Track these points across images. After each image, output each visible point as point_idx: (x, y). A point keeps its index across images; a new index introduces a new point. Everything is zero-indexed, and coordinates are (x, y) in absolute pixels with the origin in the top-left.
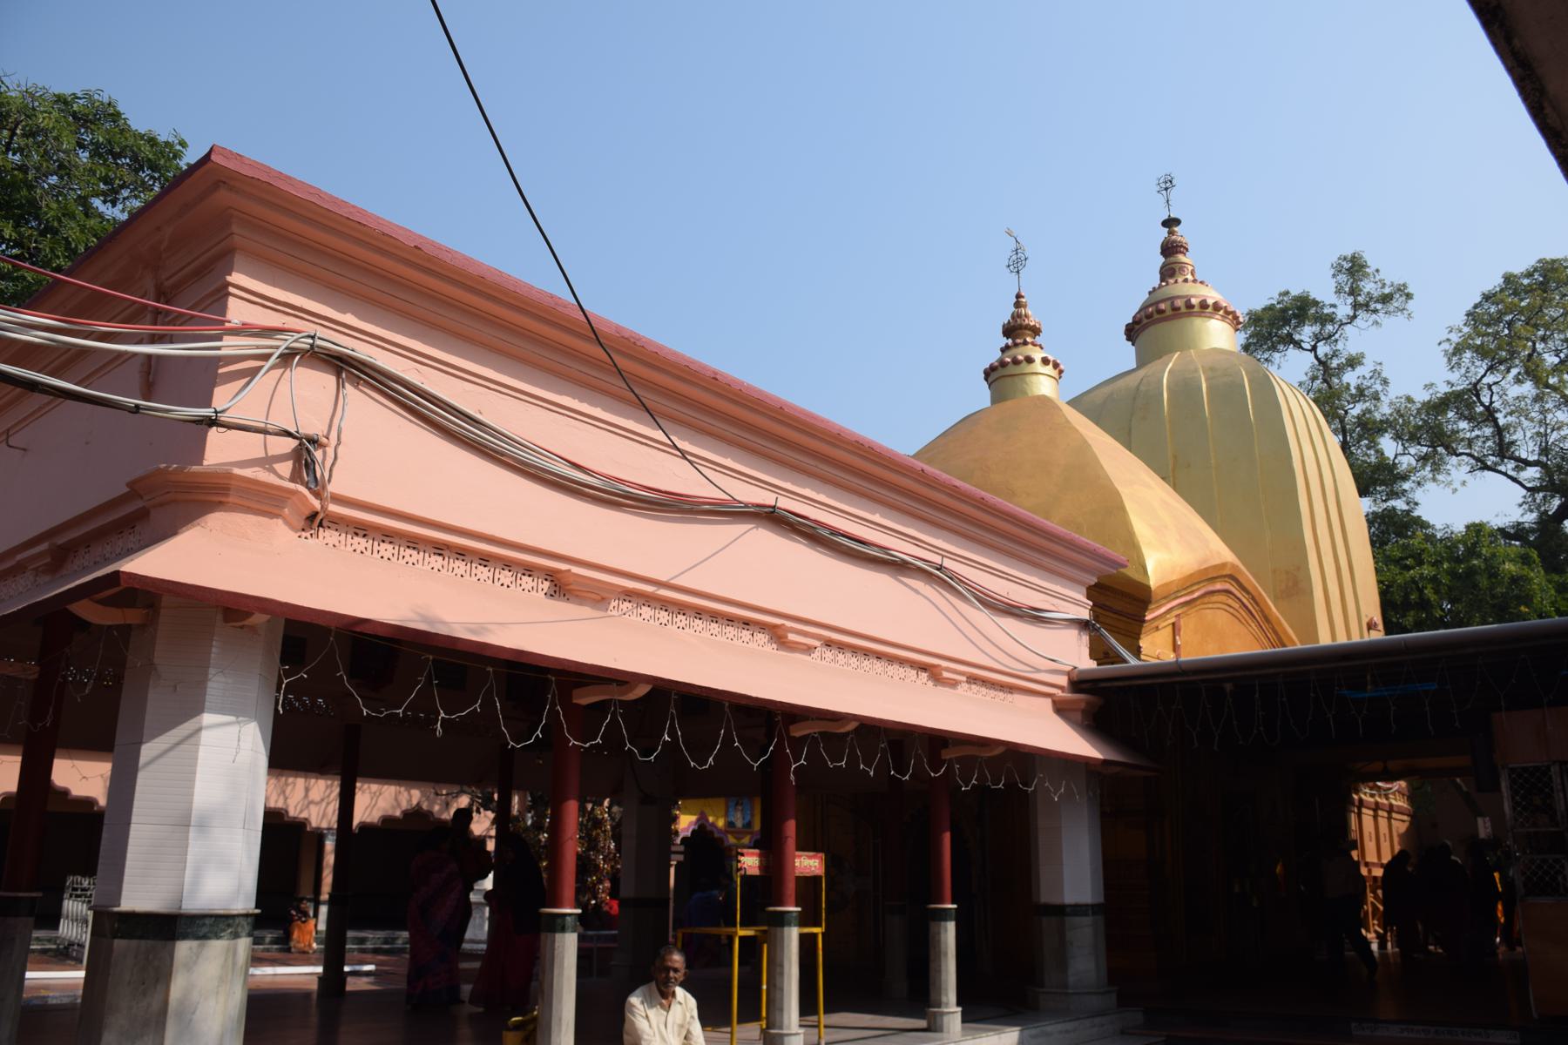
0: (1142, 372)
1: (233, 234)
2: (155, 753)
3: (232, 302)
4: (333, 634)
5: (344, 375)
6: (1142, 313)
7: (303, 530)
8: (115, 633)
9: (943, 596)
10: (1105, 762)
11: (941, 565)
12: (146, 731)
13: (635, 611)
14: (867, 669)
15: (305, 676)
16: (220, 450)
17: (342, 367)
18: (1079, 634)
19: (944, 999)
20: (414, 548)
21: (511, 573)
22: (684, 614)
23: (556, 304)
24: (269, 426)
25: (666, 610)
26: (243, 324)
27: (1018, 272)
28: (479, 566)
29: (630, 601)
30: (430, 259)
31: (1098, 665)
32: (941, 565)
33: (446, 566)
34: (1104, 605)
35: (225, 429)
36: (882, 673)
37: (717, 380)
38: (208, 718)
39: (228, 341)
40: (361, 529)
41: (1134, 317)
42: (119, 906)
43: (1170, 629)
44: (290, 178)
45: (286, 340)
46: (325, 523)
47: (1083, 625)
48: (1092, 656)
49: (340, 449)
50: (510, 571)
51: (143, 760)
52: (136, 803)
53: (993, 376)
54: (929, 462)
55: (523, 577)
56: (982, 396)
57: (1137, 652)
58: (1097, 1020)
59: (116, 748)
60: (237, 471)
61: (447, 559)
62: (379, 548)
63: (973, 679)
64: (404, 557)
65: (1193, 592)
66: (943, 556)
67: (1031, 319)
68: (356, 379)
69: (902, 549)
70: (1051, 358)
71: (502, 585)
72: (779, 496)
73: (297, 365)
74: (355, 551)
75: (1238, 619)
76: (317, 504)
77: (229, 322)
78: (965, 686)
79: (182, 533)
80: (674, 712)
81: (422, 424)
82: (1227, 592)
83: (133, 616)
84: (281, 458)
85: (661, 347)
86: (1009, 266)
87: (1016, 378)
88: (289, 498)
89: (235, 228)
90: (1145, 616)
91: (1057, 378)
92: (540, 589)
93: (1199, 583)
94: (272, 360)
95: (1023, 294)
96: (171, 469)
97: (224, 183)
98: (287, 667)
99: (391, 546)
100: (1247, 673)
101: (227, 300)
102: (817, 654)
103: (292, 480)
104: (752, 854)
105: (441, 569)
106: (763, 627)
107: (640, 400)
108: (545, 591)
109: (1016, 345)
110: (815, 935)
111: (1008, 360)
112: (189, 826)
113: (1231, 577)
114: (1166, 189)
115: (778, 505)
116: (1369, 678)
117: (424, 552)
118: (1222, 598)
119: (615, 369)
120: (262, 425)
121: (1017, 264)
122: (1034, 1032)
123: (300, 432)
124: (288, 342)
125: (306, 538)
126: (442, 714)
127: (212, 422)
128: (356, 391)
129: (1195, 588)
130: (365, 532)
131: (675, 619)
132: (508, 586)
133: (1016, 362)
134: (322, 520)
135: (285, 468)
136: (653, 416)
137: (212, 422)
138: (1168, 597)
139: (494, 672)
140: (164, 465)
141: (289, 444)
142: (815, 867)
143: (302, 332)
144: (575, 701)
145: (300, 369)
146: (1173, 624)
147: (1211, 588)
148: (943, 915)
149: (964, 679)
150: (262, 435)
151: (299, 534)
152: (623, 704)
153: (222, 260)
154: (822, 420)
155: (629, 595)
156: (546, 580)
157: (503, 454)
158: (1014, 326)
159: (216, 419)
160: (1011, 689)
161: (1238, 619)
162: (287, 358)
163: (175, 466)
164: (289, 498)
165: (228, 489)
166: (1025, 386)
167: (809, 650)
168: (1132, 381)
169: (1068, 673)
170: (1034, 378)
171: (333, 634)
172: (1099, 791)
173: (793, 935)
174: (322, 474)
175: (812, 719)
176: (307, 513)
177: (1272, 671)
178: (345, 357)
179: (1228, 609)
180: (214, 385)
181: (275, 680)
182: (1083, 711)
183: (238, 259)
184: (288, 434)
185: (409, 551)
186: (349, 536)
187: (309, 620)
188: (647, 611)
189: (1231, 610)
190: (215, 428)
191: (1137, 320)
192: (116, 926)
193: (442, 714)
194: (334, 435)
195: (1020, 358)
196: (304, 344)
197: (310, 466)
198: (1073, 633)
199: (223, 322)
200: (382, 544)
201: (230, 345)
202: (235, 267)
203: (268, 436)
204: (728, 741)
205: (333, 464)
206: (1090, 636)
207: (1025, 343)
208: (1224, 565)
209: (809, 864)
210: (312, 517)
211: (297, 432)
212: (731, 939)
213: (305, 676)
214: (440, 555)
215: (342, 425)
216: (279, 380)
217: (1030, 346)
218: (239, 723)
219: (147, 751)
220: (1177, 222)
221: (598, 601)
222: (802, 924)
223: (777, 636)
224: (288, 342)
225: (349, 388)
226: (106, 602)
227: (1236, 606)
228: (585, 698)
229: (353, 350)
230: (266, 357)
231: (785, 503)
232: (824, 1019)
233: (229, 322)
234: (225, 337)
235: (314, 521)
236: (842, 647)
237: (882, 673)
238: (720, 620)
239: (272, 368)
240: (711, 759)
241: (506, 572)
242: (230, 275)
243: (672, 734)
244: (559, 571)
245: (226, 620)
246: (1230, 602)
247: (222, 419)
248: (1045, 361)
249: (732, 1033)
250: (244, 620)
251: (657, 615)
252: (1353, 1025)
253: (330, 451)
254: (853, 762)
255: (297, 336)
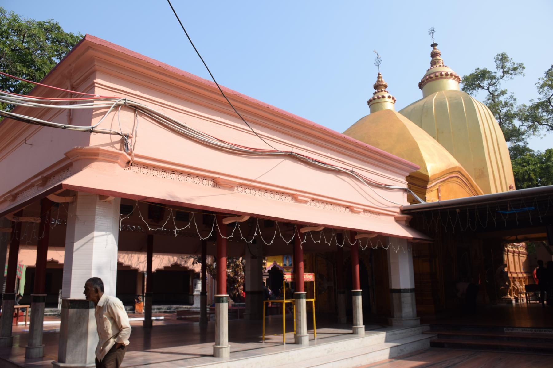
0: (425, 100)
1: (95, 65)
2: (79, 246)
3: (96, 89)
4: (137, 202)
5: (137, 112)
6: (425, 78)
7: (126, 167)
8: (63, 205)
9: (355, 182)
10: (414, 239)
11: (352, 171)
12: (75, 239)
13: (243, 191)
14: (327, 208)
15: (128, 217)
16: (95, 141)
17: (136, 110)
18: (403, 193)
19: (358, 323)
20: (165, 172)
21: (199, 179)
22: (261, 191)
23: (210, 84)
24: (112, 131)
25: (255, 190)
26: (100, 96)
27: (378, 65)
28: (188, 177)
29: (242, 187)
30: (164, 70)
31: (411, 204)
32: (352, 171)
33: (176, 177)
34: (413, 183)
35: (96, 133)
36: (333, 210)
37: (269, 108)
38: (96, 233)
39: (96, 102)
40: (146, 166)
41: (422, 80)
42: (70, 297)
43: (437, 190)
44: (114, 44)
45: (116, 101)
46: (133, 164)
47: (405, 190)
48: (408, 201)
49: (137, 138)
50: (199, 178)
51: (75, 248)
52: (73, 263)
53: (371, 103)
54: (349, 135)
55: (203, 180)
56: (366, 110)
57: (425, 199)
58: (413, 329)
59: (66, 245)
60: (101, 148)
61: (176, 175)
62: (152, 172)
63: (365, 211)
64: (161, 175)
66: (353, 167)
67: (384, 82)
68: (141, 114)
69: (338, 165)
70: (391, 96)
72: (293, 148)
73: (120, 110)
74: (144, 173)
75: (461, 186)
76: (130, 158)
77: (95, 96)
78: (363, 213)
79: (84, 169)
80: (258, 225)
81: (166, 129)
82: (457, 177)
83: (68, 199)
84: (116, 143)
85: (248, 97)
86: (375, 64)
87: (379, 104)
88: (119, 156)
89: (96, 63)
90: (427, 186)
91: (394, 102)
92: (209, 184)
93: (446, 174)
94: (111, 109)
95: (380, 73)
96: (78, 148)
97: (91, 47)
98: (122, 215)
99: (156, 171)
100: (464, 205)
101: (94, 88)
102: (309, 203)
103: (121, 149)
104: (288, 274)
105: (174, 178)
106: (289, 195)
107: (240, 116)
108: (211, 185)
109: (378, 92)
110: (312, 302)
111: (376, 97)
113: (459, 172)
114: (432, 33)
115: (293, 151)
116: (508, 205)
117: (168, 173)
119: (230, 105)
120: (109, 131)
121: (378, 63)
122: (390, 333)
123: (122, 133)
124: (116, 102)
125: (127, 170)
126: (177, 229)
127: (91, 131)
128: (141, 118)
129: (445, 176)
130: (147, 167)
131: (258, 193)
132: (198, 184)
133: (379, 98)
134: (132, 164)
135: (118, 146)
136: (245, 121)
137: (91, 131)
138: (435, 180)
139: (194, 213)
140: (76, 147)
141: (119, 138)
142: (311, 278)
143: (121, 99)
144: (224, 223)
145: (121, 111)
146: (438, 189)
147: (451, 176)
148: (357, 294)
149: (362, 210)
150: (109, 135)
151: (124, 168)
152: (240, 223)
153: (92, 74)
154: (308, 121)
155: (241, 185)
156: (212, 181)
157: (194, 138)
158: (378, 85)
159: (93, 130)
160: (379, 214)
161: (461, 186)
162: (116, 107)
163: (80, 147)
164: (119, 156)
165: (98, 154)
166: (382, 106)
167: (306, 202)
168: (421, 103)
169: (400, 208)
170: (385, 103)
171: (137, 202)
172: (412, 249)
173: (304, 302)
174: (131, 148)
175: (308, 226)
176: (127, 161)
177: (473, 204)
178: (137, 106)
179: (458, 183)
180: (92, 118)
181: (119, 220)
182: (406, 221)
183: (98, 74)
184: (118, 134)
185: (163, 173)
186: (142, 169)
187: (128, 198)
188: (247, 190)
189: (459, 183)
190: (92, 133)
191: (423, 81)
192: (69, 304)
193: (177, 229)
194: (134, 134)
195: (380, 96)
196: (122, 102)
197: (126, 144)
198: (401, 193)
199: (93, 96)
200: (153, 171)
201: (97, 104)
202: (97, 77)
203: (111, 135)
204: (278, 235)
205: (135, 144)
206: (407, 194)
207: (382, 91)
208: (456, 167)
209: (309, 277)
210: (128, 162)
211: (121, 133)
212: (282, 304)
213: (128, 217)
214: (174, 174)
215: (137, 130)
216: (114, 115)
217: (384, 92)
218: (107, 235)
219: (76, 245)
220: (436, 45)
221: (231, 188)
222: (307, 298)
223: (295, 198)
224: (116, 102)
225: (139, 117)
226: (59, 195)
227: (461, 182)
228: (227, 222)
229: (139, 104)
230: (109, 108)
231: (295, 151)
232: (316, 331)
233: (95, 96)
234: (95, 101)
235: (129, 164)
236: (318, 201)
237: (333, 210)
238: (274, 193)
239: (112, 111)
240: (272, 241)
241: (197, 179)
242: (95, 79)
243: (258, 233)
244: (216, 178)
245: (100, 199)
246: (458, 180)
247: (95, 130)
248: (389, 97)
249: (283, 336)
250: (106, 199)
251: (251, 192)
252: (505, 329)
253: (133, 139)
254: (323, 241)
255: (119, 99)
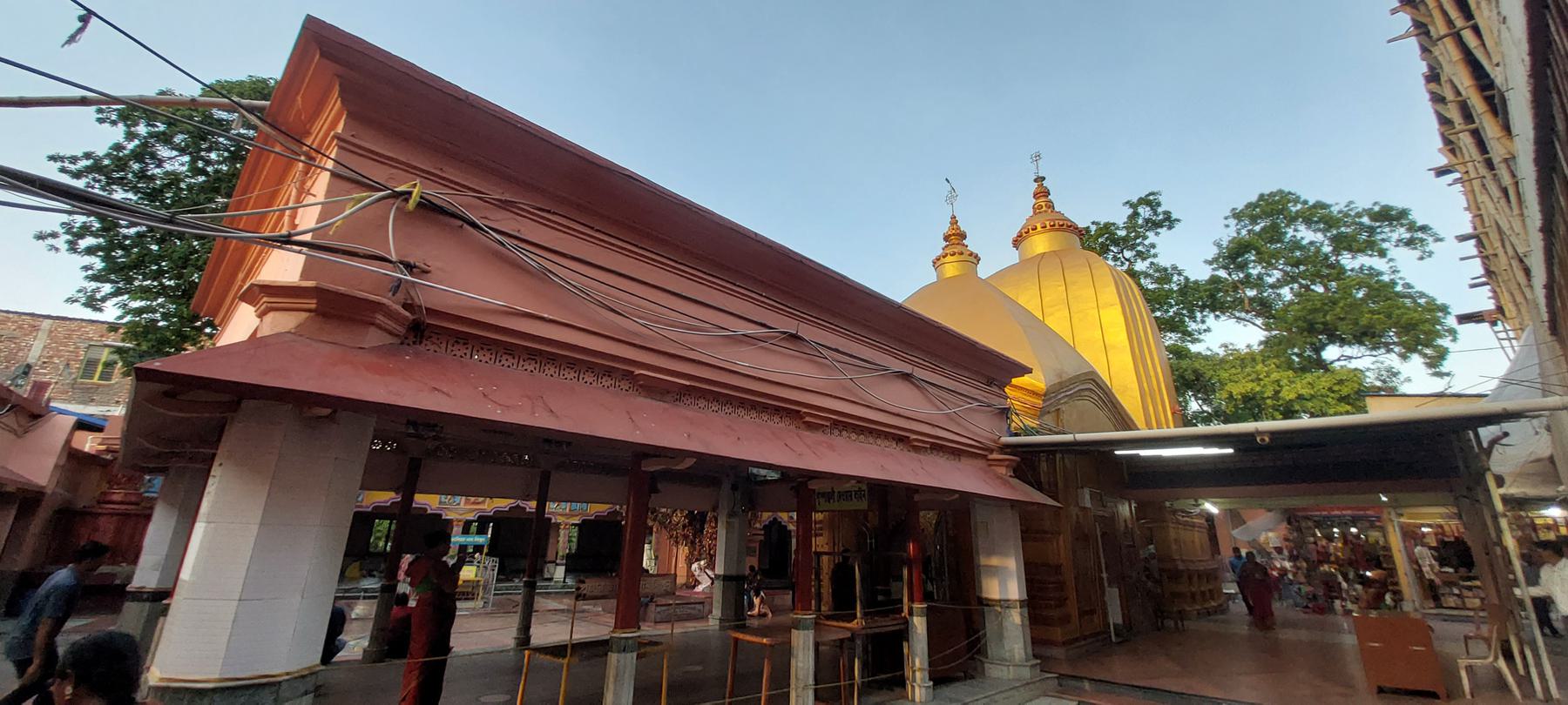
53: (939, 263)
65: (1071, 390)
71: (586, 382)
82: (1091, 390)
112: (240, 600)
118: (1087, 393)
121: (952, 196)
129: (1071, 387)
144: (643, 469)
220: (1044, 179)
